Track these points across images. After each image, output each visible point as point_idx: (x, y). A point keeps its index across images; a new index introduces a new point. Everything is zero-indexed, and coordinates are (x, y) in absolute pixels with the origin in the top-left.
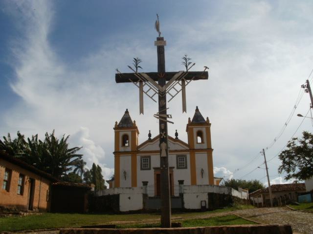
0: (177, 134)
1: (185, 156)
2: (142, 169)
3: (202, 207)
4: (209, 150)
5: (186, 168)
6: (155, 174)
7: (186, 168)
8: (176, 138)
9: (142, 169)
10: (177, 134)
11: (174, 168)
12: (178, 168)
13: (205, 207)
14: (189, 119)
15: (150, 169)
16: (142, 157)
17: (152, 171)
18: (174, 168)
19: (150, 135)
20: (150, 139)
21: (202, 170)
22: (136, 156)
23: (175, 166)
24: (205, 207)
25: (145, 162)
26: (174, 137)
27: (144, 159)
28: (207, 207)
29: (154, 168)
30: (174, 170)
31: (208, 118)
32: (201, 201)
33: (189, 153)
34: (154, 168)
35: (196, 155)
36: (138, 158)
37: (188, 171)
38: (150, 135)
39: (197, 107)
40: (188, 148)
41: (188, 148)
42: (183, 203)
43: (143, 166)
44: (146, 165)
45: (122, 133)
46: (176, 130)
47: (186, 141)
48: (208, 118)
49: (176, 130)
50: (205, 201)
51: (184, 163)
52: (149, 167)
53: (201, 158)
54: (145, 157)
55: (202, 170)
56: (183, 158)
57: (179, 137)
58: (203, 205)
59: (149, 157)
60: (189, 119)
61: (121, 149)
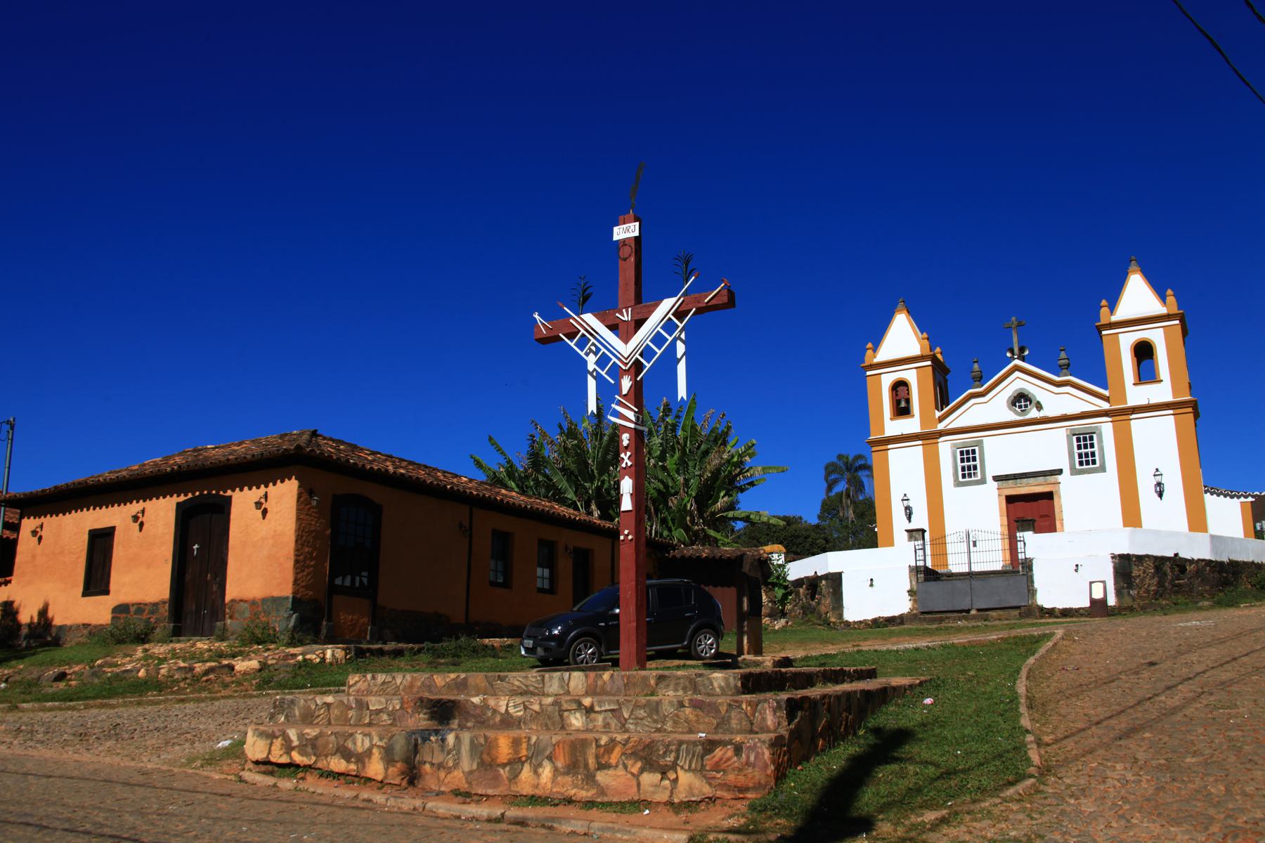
2: (958, 484)
3: (1093, 601)
5: (1102, 469)
7: (1102, 469)
11: (1060, 472)
12: (1074, 472)
13: (1103, 601)
15: (983, 481)
17: (992, 486)
18: (1060, 472)
21: (1157, 473)
23: (1064, 464)
24: (1103, 601)
25: (968, 460)
27: (962, 453)
28: (1112, 601)
29: (996, 478)
30: (1060, 478)
32: (1091, 583)
34: (996, 478)
40: (1105, 406)
42: (1032, 592)
43: (960, 473)
44: (969, 468)
51: (1093, 454)
55: (1157, 473)
56: (1091, 438)
58: (1098, 594)
59: (980, 444)
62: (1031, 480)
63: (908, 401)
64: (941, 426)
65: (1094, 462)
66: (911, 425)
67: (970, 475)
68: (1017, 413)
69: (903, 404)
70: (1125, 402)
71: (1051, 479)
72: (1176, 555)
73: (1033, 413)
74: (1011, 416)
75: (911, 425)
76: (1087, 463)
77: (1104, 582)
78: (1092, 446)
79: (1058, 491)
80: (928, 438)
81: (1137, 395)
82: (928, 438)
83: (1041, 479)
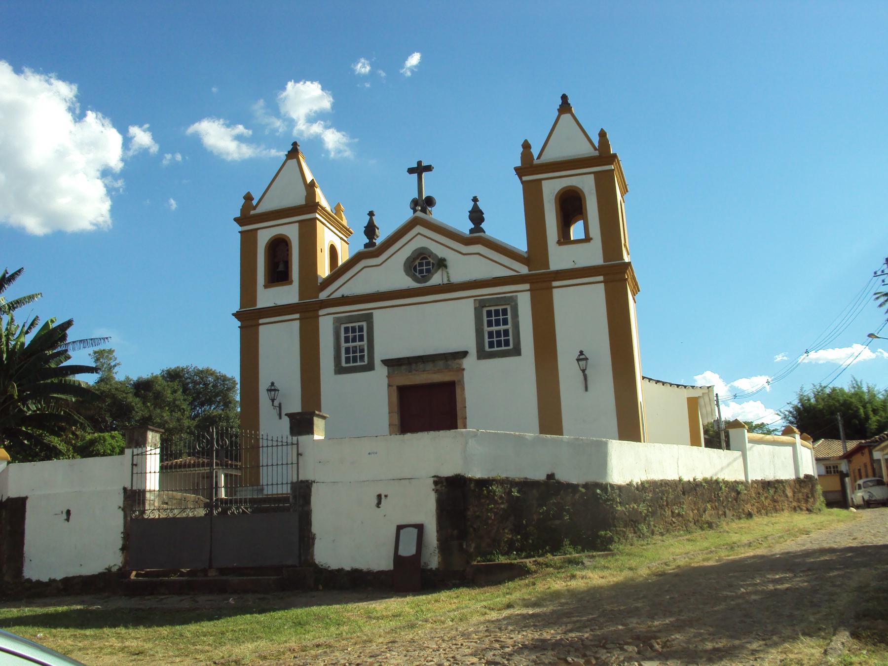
0: (477, 216)
1: (512, 302)
2: (340, 370)
4: (615, 276)
5: (517, 351)
6: (389, 386)
7: (517, 351)
8: (472, 231)
9: (340, 370)
10: (477, 216)
11: (464, 354)
12: (482, 355)
14: (526, 146)
15: (370, 367)
16: (338, 322)
17: (381, 372)
18: (464, 354)
19: (370, 230)
20: (371, 244)
21: (582, 358)
22: (318, 316)
23: (469, 342)
26: (465, 227)
27: (347, 330)
28: (433, 560)
29: (386, 362)
31: (602, 135)
32: (400, 528)
33: (527, 286)
34: (386, 362)
35: (556, 293)
36: (326, 324)
37: (524, 365)
38: (370, 230)
39: (564, 98)
40: (524, 270)
41: (524, 270)
42: (306, 539)
45: (264, 237)
46: (475, 200)
47: (520, 243)
48: (602, 135)
49: (475, 200)
50: (420, 528)
51: (506, 332)
52: (344, 364)
53: (579, 311)
54: (351, 319)
55: (582, 358)
56: (505, 312)
57: (490, 229)
58: (408, 549)
59: (369, 318)
60: (526, 146)
61: (267, 297)
62: (430, 366)
63: (287, 264)
64: (323, 295)
65: (507, 343)
66: (288, 294)
67: (355, 361)
68: (416, 280)
69: (281, 267)
70: (548, 267)
71: (453, 364)
72: (551, 476)
73: (437, 279)
74: (408, 283)
75: (288, 294)
76: (499, 345)
77: (420, 528)
78: (505, 322)
79: (461, 382)
80: (307, 311)
81: (560, 258)
82: (307, 311)
83: (441, 364)
